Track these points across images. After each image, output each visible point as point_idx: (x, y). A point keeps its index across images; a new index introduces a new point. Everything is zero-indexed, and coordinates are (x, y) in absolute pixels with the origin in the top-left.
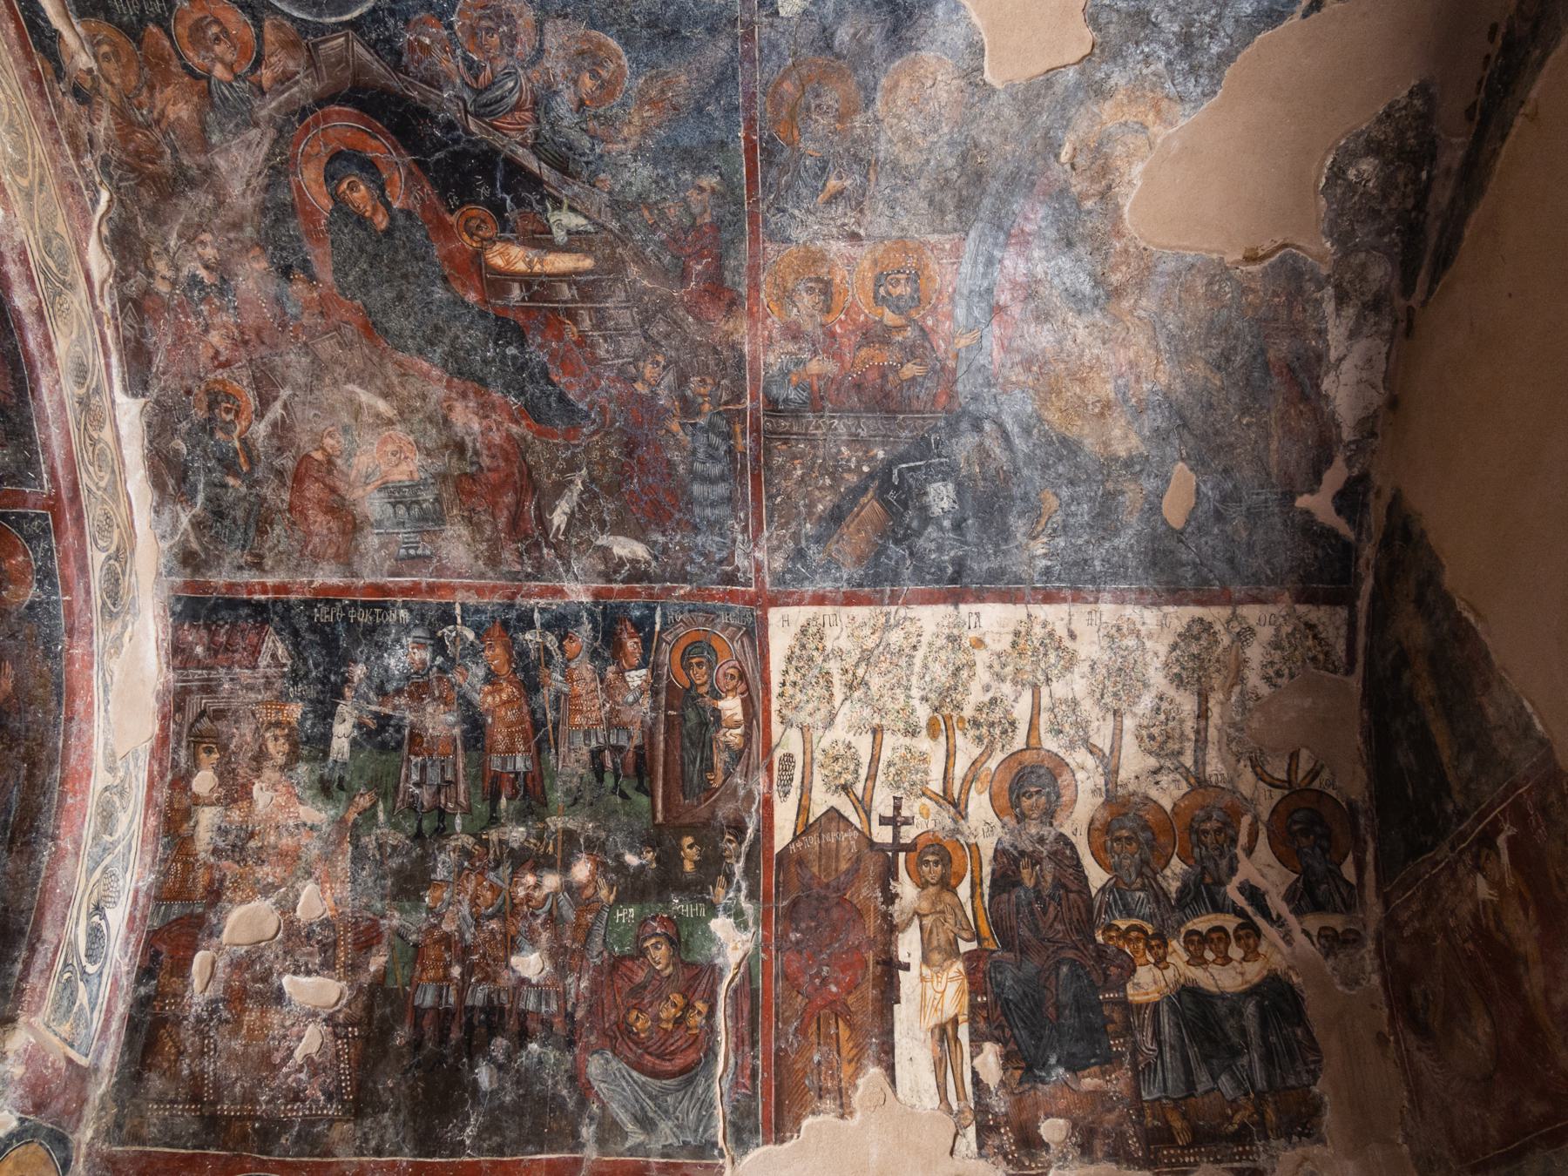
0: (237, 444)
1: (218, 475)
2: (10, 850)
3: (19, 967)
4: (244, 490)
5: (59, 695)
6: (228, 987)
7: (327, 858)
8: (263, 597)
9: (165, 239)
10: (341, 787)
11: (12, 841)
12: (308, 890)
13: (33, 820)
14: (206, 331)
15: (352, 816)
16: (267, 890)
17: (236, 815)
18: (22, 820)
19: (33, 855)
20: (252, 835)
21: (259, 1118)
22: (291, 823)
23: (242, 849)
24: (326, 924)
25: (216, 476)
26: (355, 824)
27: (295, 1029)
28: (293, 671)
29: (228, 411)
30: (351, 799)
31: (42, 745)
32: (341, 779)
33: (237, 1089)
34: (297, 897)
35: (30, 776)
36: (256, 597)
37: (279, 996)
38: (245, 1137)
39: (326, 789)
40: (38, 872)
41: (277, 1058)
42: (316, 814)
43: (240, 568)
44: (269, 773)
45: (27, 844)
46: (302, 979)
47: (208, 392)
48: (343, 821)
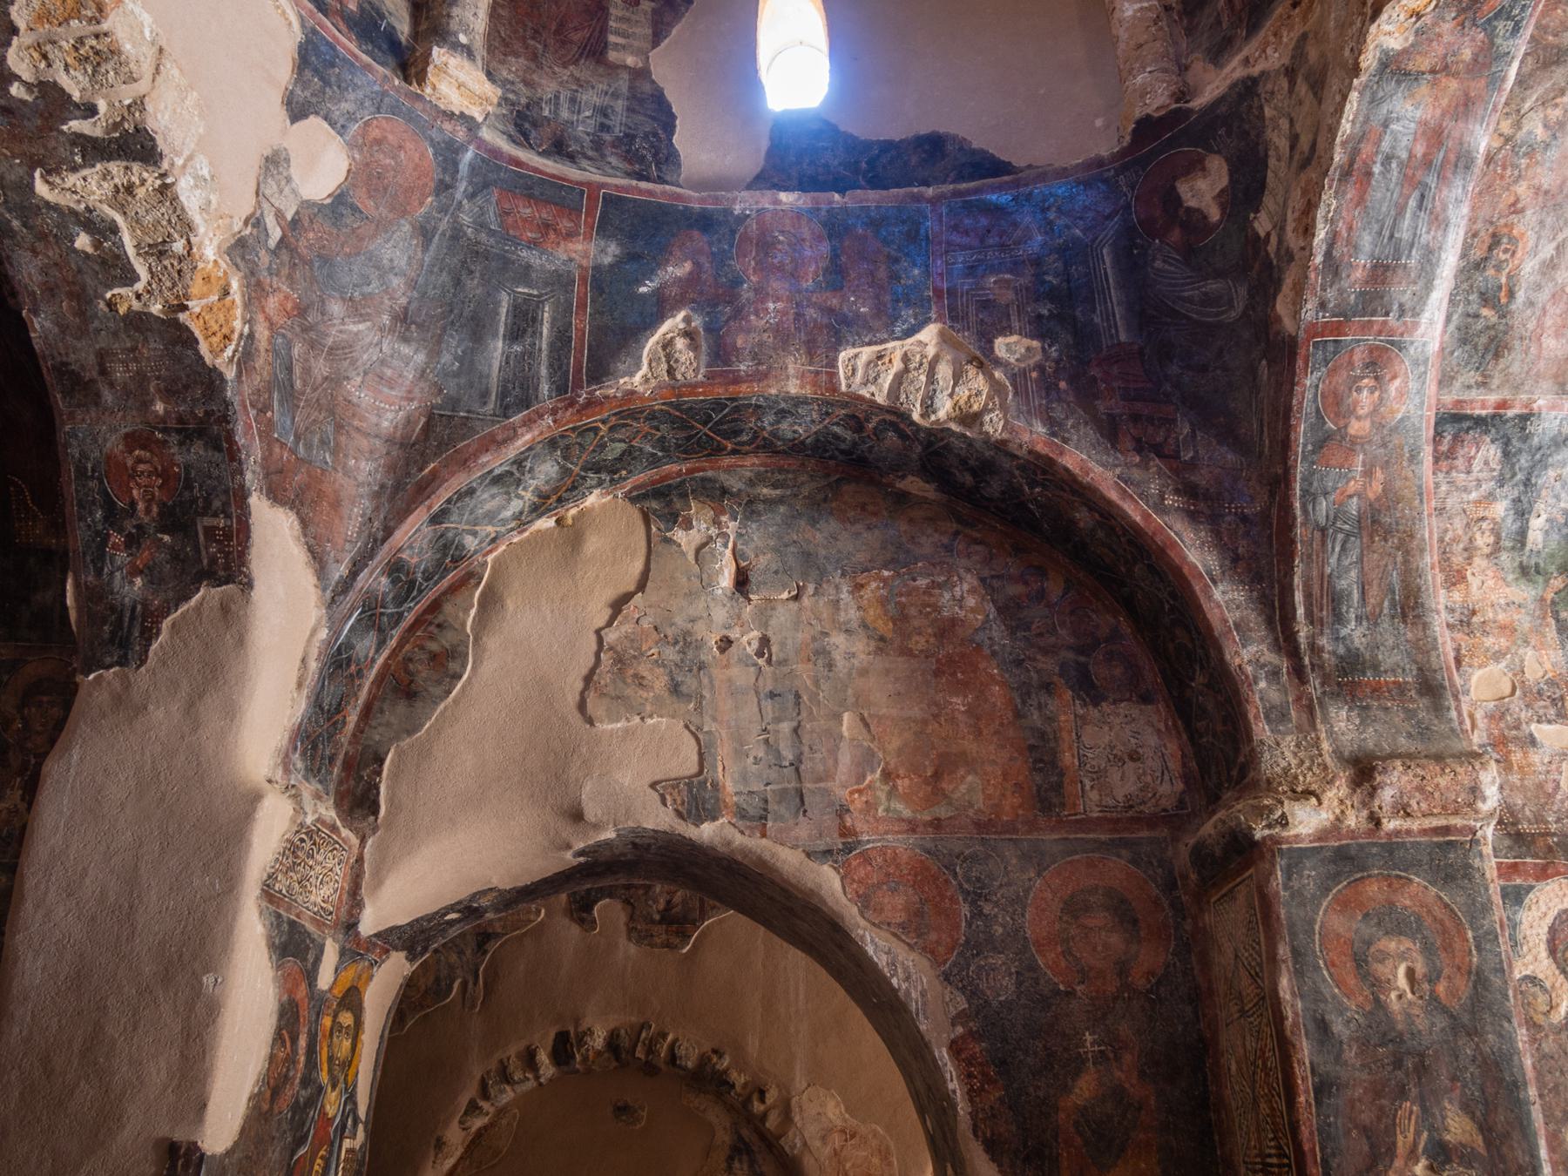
0: (1504, 280)
1: (1475, 306)
2: (1405, 622)
3: (1454, 714)
4: (1494, 319)
5: (1421, 494)
6: (1490, 735)
7: (1537, 630)
8: (1484, 413)
9: (1523, 100)
10: (1538, 572)
11: (1404, 616)
12: (1529, 654)
13: (1416, 598)
14: (1516, 181)
15: (1550, 596)
16: (1498, 656)
17: (1457, 596)
18: (1407, 598)
19: (1426, 626)
20: (1474, 613)
21: (1554, 834)
22: (1502, 601)
23: (1469, 624)
24: (1551, 683)
25: (1472, 309)
26: (1553, 602)
27: (1554, 767)
28: (1501, 474)
29: (1506, 251)
30: (1547, 581)
31: (1412, 536)
32: (1537, 565)
33: (1528, 813)
34: (1522, 661)
35: (1406, 562)
36: (1477, 412)
37: (1532, 741)
38: (1550, 849)
39: (1525, 572)
40: (1435, 639)
41: (1549, 788)
42: (1525, 593)
43: (1469, 387)
44: (1479, 562)
45: (1418, 617)
46: (1545, 727)
47: (1494, 235)
48: (1542, 599)
